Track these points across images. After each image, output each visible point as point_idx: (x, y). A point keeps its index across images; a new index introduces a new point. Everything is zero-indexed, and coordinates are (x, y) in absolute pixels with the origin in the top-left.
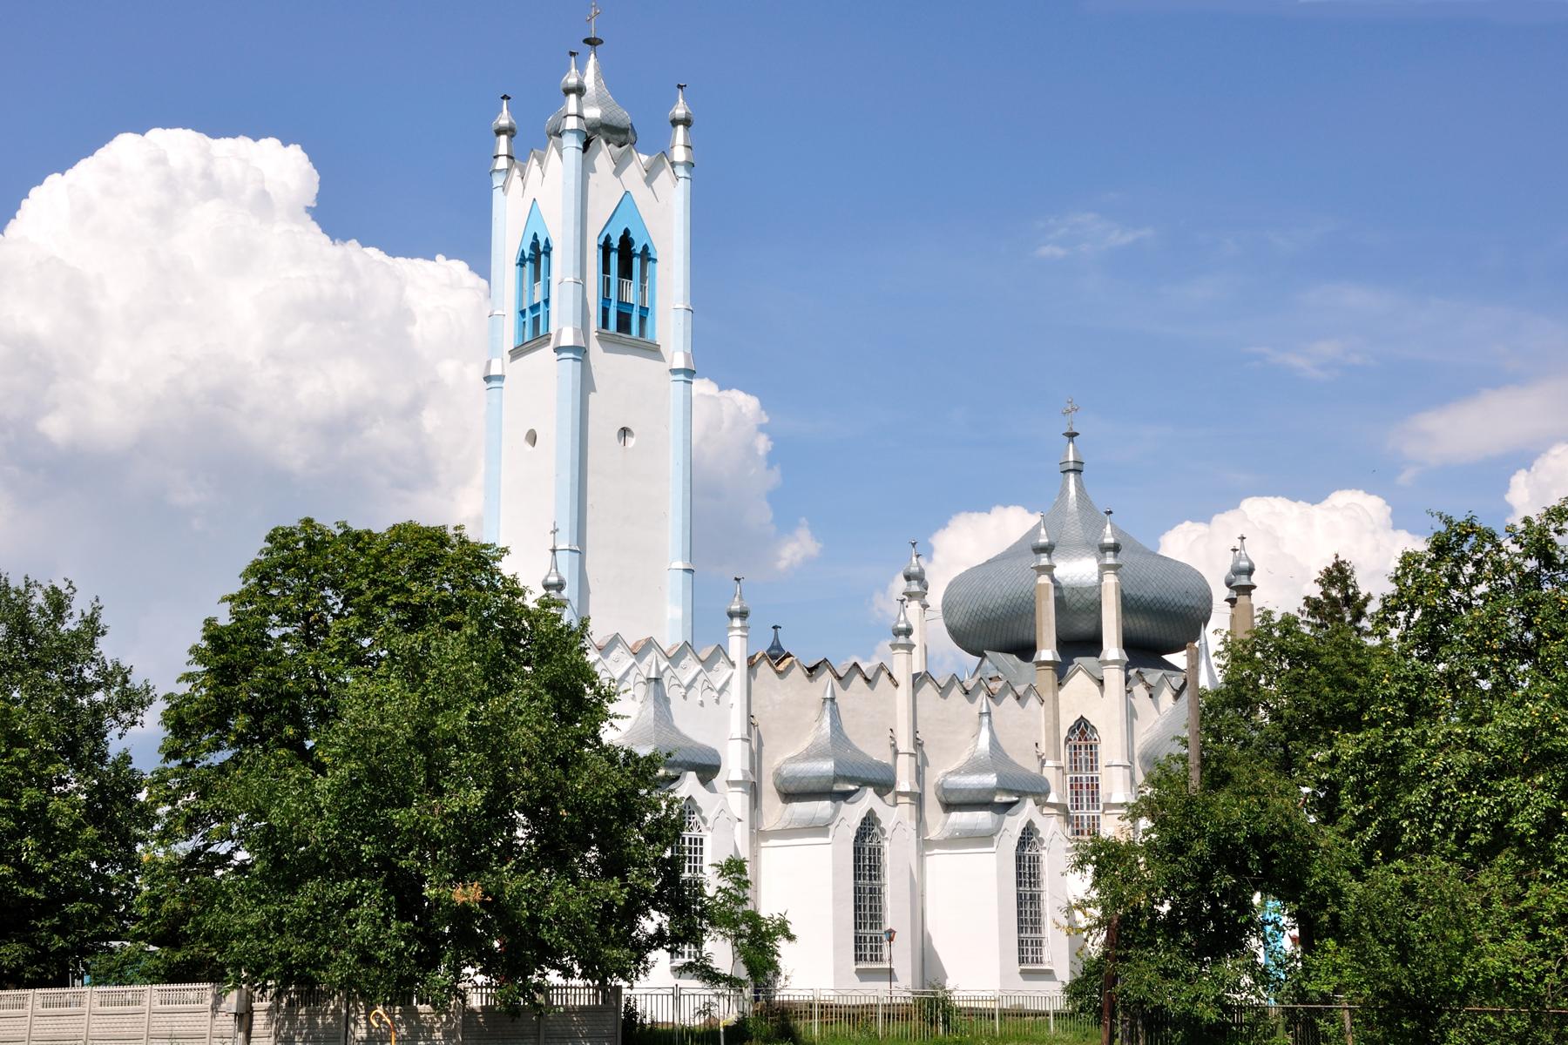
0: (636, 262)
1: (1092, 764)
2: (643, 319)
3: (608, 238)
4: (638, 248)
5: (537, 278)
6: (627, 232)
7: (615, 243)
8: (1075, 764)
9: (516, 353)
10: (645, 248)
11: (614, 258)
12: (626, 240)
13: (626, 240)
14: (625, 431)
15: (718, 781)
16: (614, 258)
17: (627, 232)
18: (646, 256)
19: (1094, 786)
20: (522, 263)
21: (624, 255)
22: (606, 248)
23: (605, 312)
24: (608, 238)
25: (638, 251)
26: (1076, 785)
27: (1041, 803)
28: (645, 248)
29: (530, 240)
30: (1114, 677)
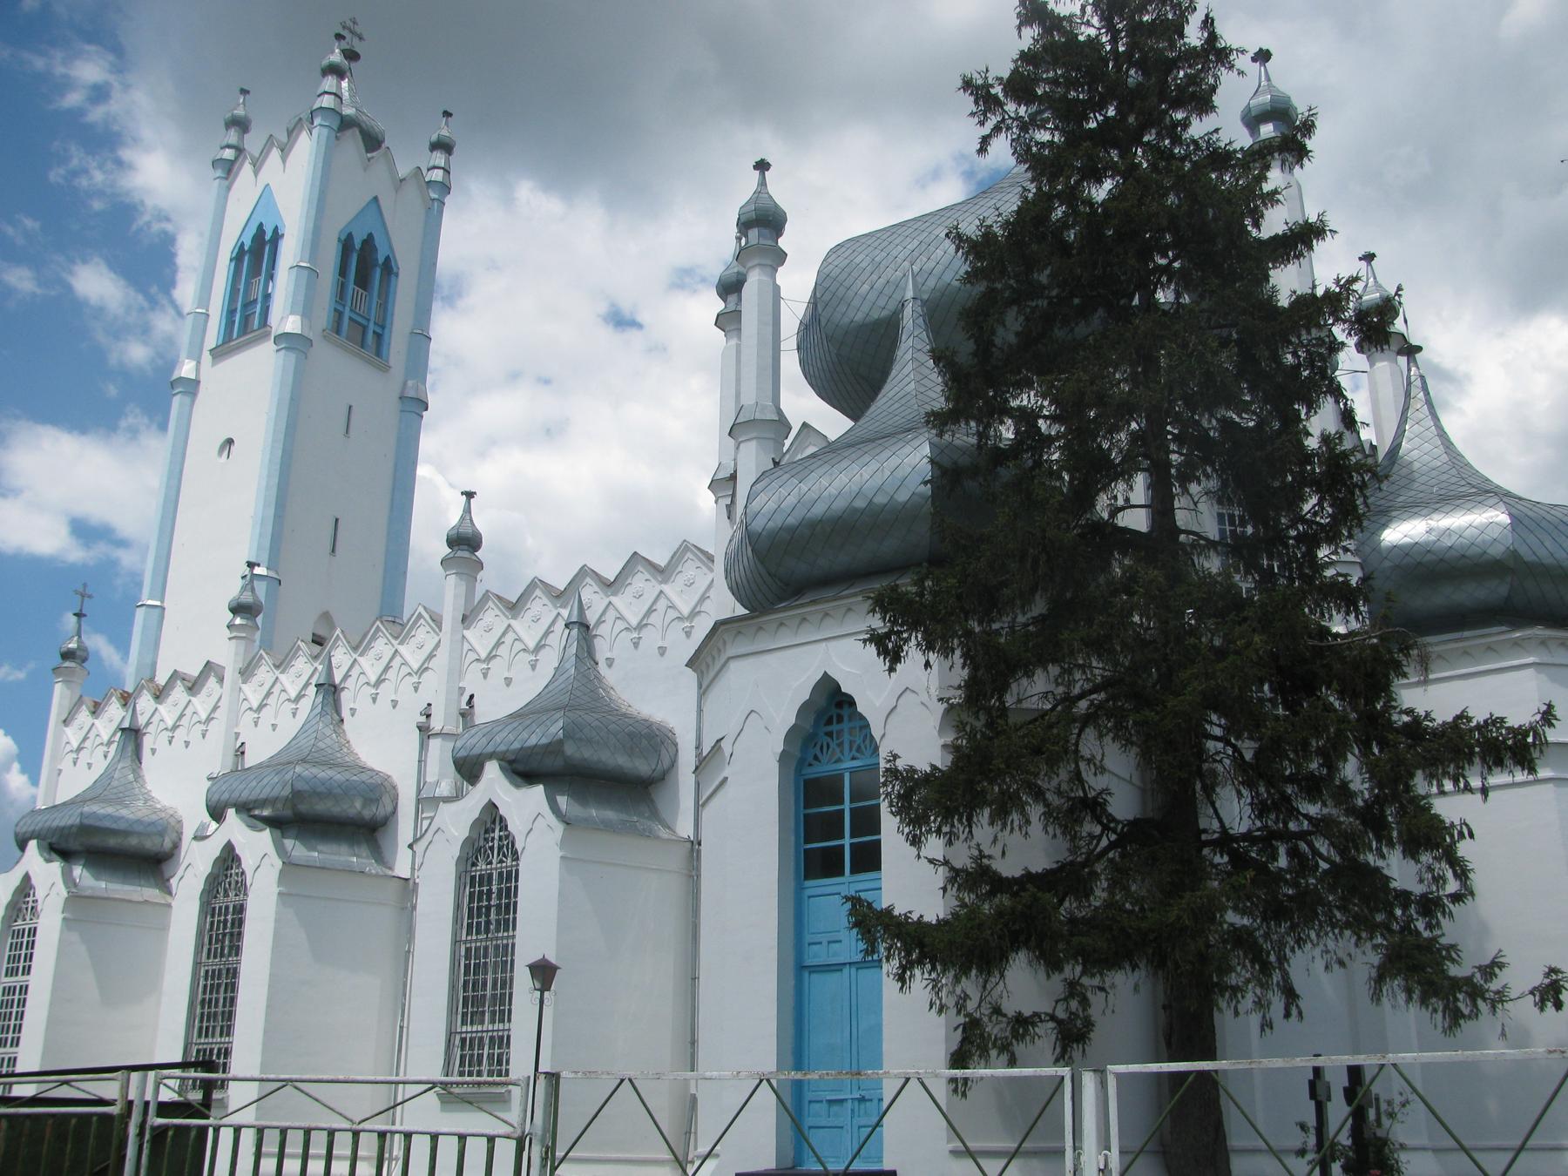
0: (378, 271)
2: (379, 337)
3: (350, 236)
5: (255, 271)
6: (370, 236)
7: (358, 245)
9: (219, 353)
10: (388, 259)
12: (369, 242)
13: (369, 242)
17: (370, 236)
18: (389, 269)
20: (238, 258)
22: (346, 245)
24: (350, 236)
25: (381, 260)
29: (252, 230)
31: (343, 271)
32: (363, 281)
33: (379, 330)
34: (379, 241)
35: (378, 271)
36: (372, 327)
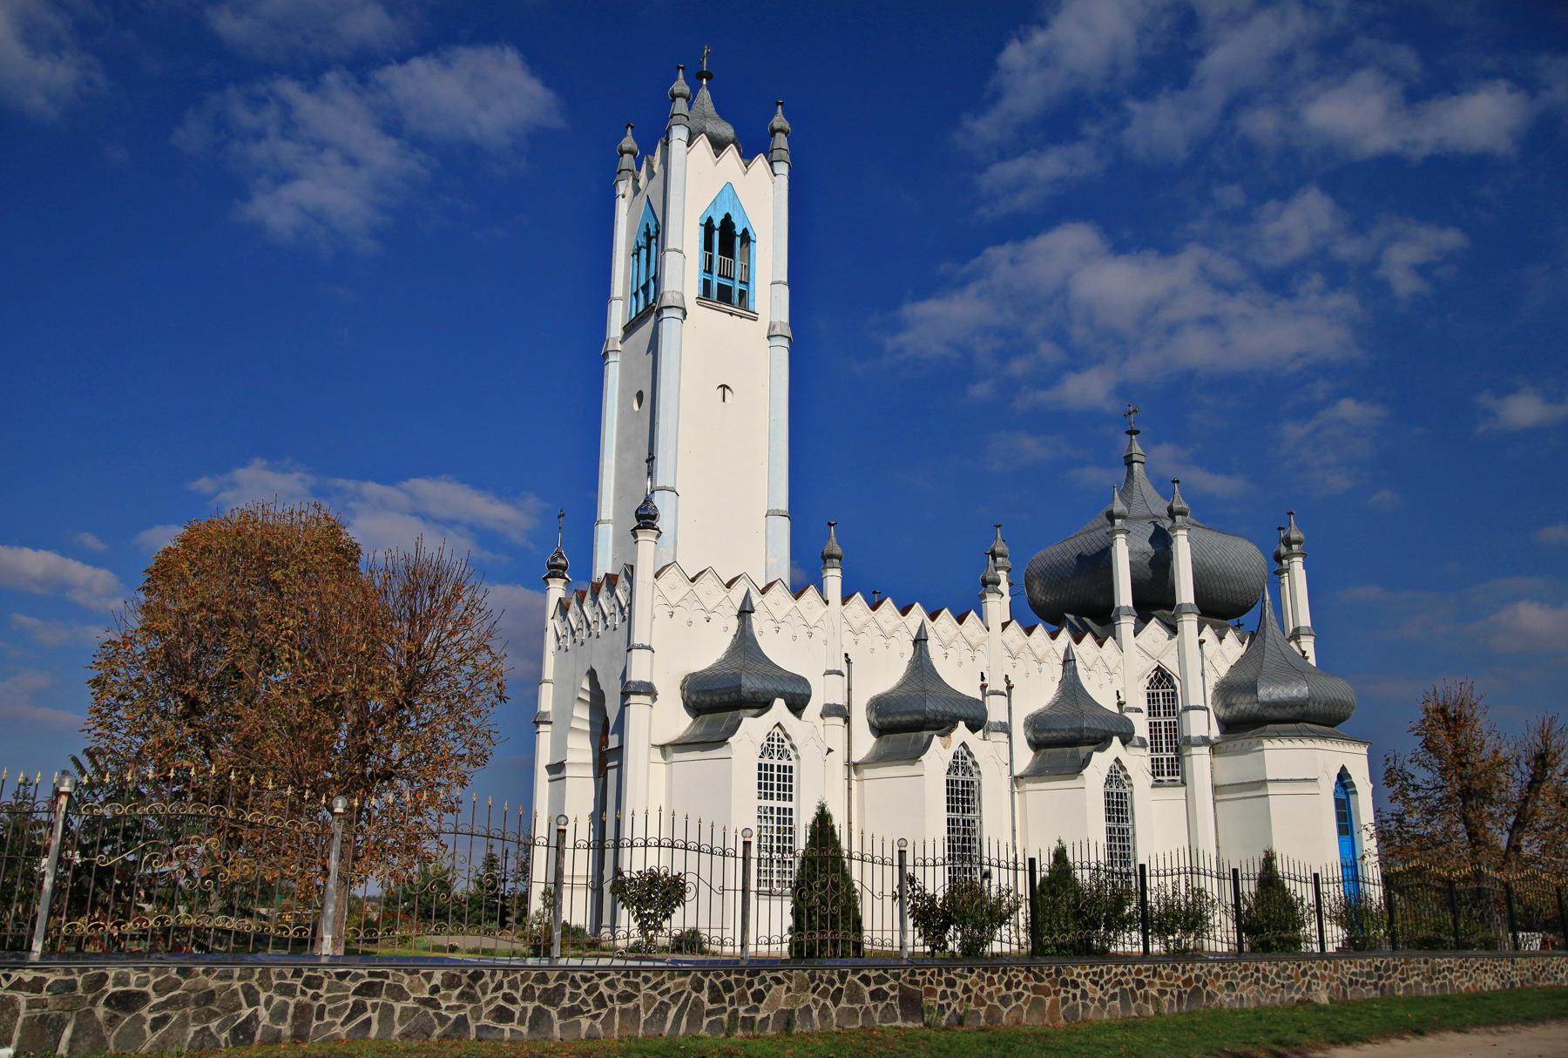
0: (738, 240)
1: (1171, 709)
2: (742, 294)
3: (710, 220)
4: (739, 231)
6: (728, 216)
7: (717, 224)
8: (1153, 711)
10: (745, 231)
11: (717, 234)
13: (727, 222)
14: (724, 387)
15: (813, 709)
16: (717, 234)
17: (728, 216)
18: (746, 238)
19: (1173, 729)
20: (637, 252)
21: (725, 238)
22: (708, 227)
23: (707, 285)
24: (710, 220)
26: (1154, 728)
27: (1126, 740)
28: (745, 231)
30: (1189, 623)
33: (743, 287)
35: (738, 240)
36: (738, 287)
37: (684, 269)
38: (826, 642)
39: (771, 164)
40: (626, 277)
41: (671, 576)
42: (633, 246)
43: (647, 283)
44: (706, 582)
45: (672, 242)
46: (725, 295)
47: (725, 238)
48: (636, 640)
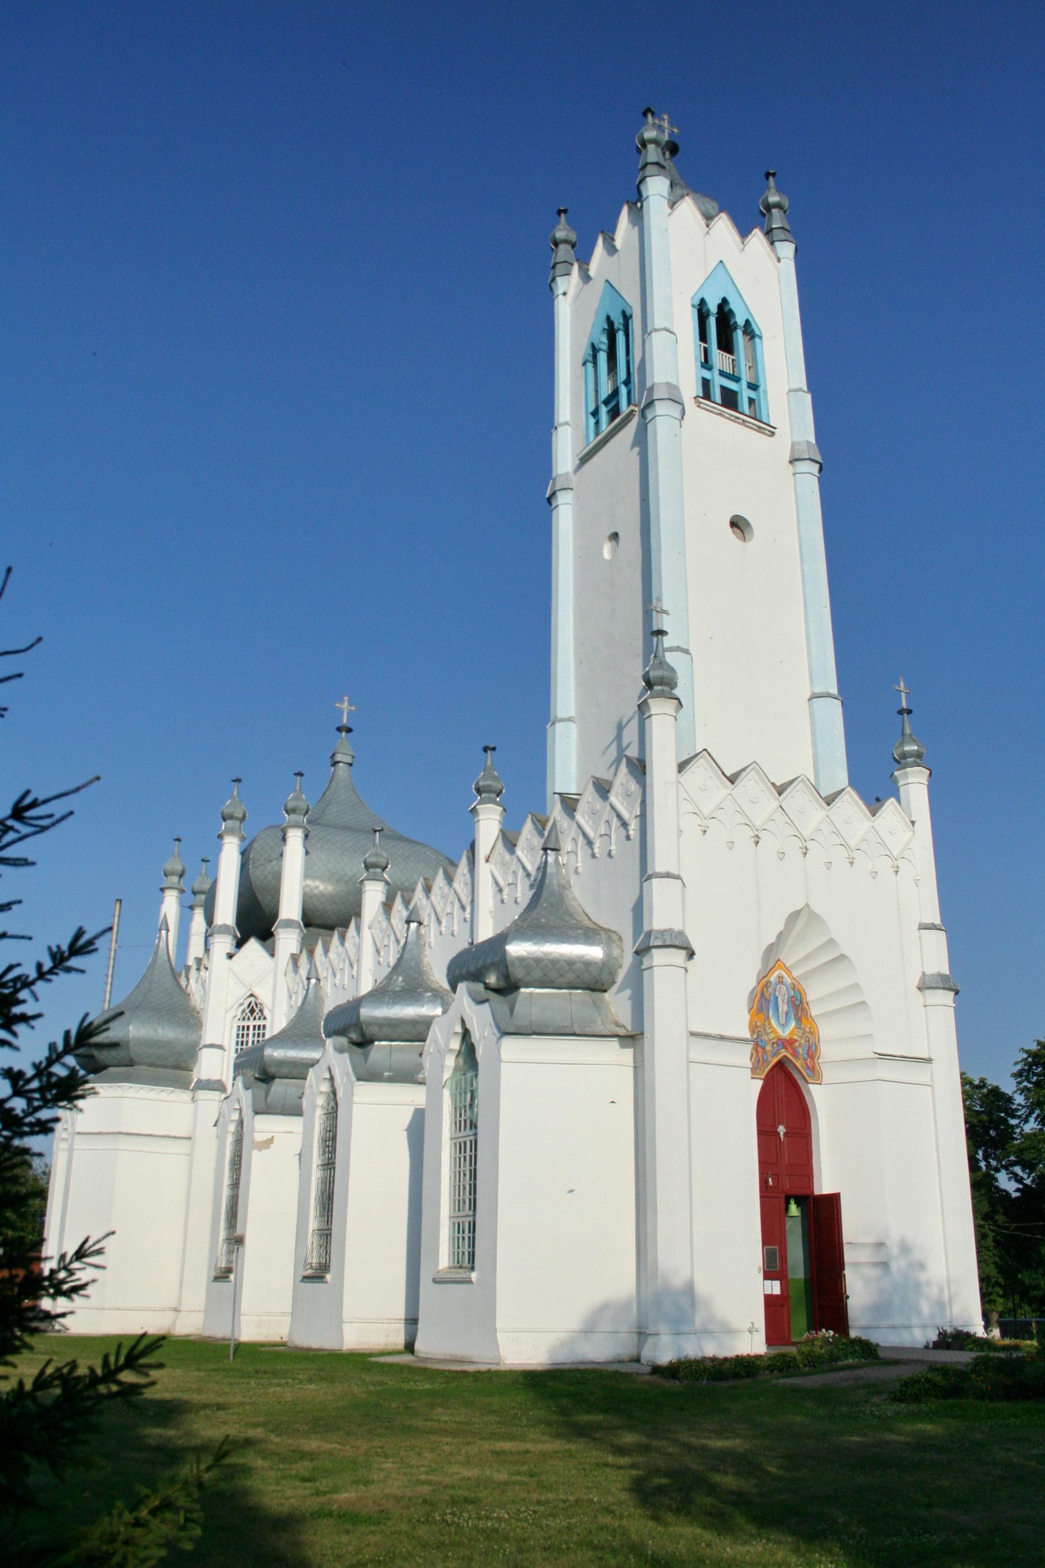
3: (703, 302)
4: (740, 320)
6: (725, 301)
7: (713, 307)
10: (747, 322)
17: (725, 301)
18: (749, 330)
21: (722, 327)
23: (706, 384)
24: (703, 302)
28: (747, 322)
31: (703, 336)
32: (726, 345)
34: (734, 305)
37: (673, 355)
38: (917, 882)
39: (772, 243)
40: (574, 394)
41: (699, 769)
42: (584, 350)
43: (615, 393)
44: (749, 784)
45: (658, 320)
46: (730, 400)
47: (722, 327)
48: (660, 863)
